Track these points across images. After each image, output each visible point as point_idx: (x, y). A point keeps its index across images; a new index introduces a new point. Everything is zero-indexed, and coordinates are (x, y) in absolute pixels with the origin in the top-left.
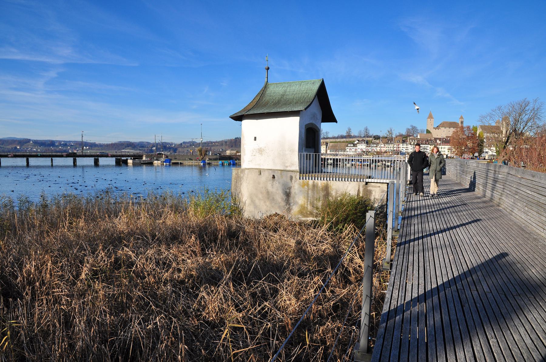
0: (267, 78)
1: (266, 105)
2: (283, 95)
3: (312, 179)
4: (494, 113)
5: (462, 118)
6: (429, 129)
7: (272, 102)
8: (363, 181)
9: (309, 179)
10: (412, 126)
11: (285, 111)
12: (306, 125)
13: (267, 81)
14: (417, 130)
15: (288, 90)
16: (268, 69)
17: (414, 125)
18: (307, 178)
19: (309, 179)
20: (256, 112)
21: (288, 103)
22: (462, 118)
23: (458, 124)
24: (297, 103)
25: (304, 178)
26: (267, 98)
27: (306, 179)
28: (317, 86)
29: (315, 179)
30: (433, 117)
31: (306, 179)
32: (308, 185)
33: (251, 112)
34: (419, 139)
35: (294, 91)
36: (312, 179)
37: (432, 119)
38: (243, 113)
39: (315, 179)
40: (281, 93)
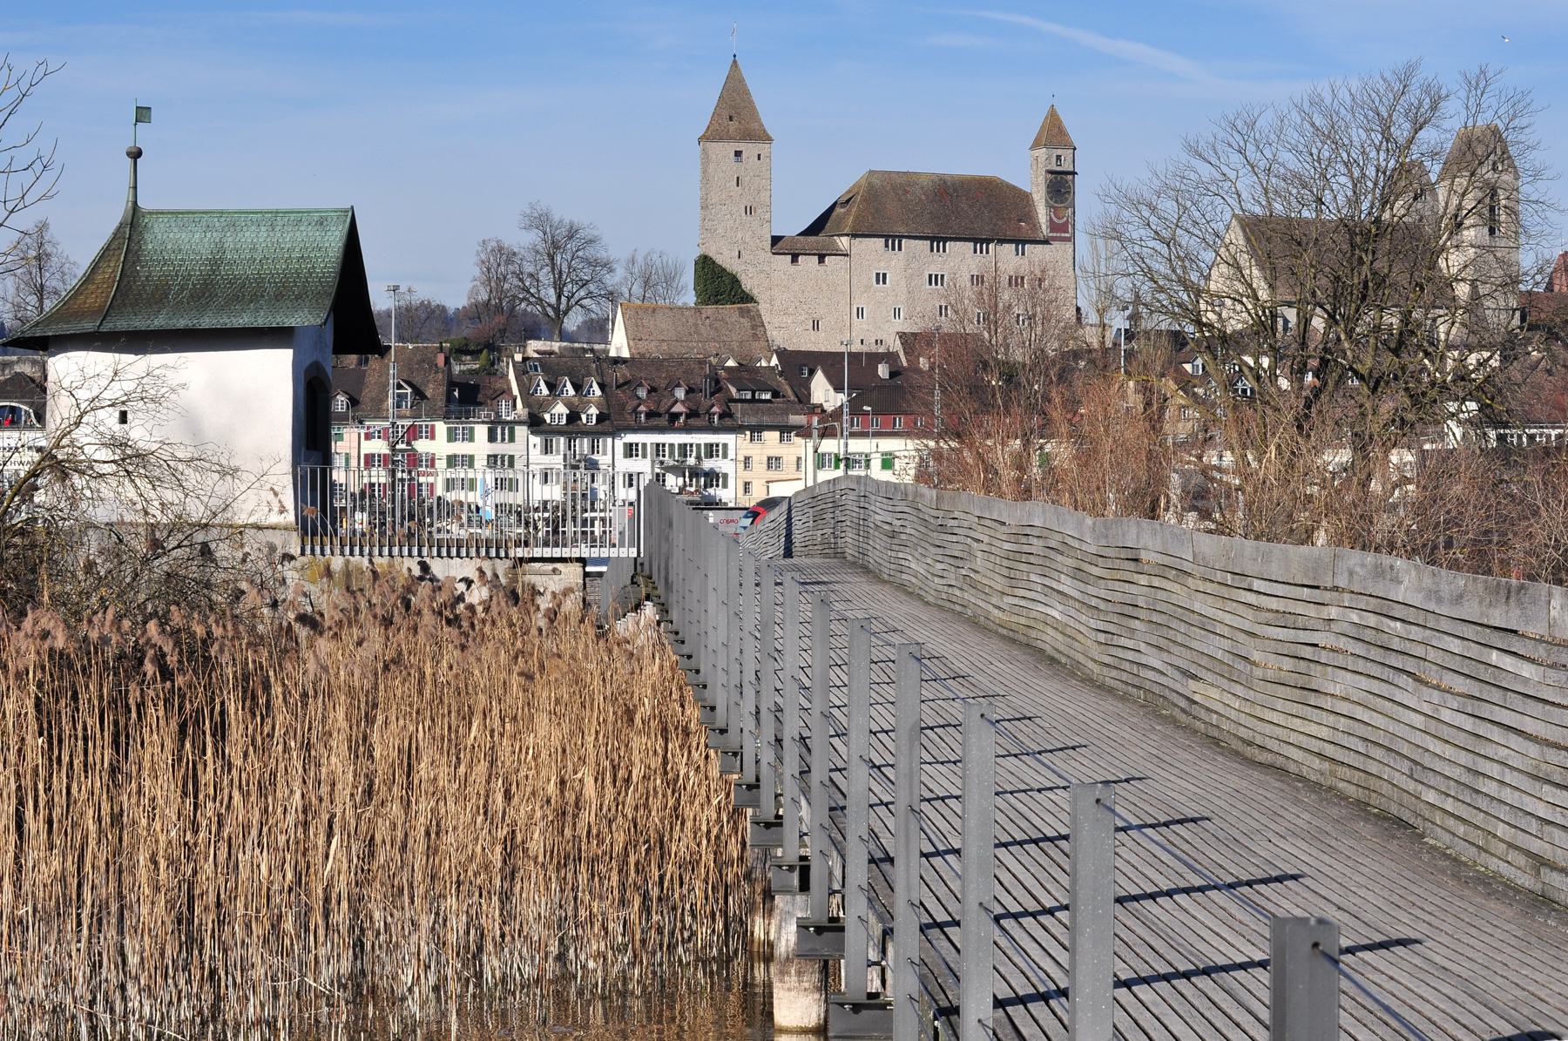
0: (135, 188)
1: (159, 297)
2: (215, 263)
3: (342, 554)
4: (1206, 171)
5: (1054, 134)
6: (726, 259)
7: (182, 289)
8: (507, 557)
9: (332, 554)
10: (540, 221)
11: (255, 325)
12: (306, 371)
13: (135, 203)
14: (594, 263)
15: (229, 243)
16: (136, 155)
17: (565, 212)
18: (328, 551)
19: (332, 554)
20: (139, 323)
21: (246, 291)
22: (1054, 134)
23: (1021, 200)
24: (279, 297)
25: (318, 549)
26: (156, 271)
27: (323, 554)
28: (337, 233)
29: (352, 554)
30: (769, 122)
31: (323, 554)
32: (328, 572)
33: (121, 324)
34: (622, 373)
35: (254, 249)
36: (342, 554)
37: (749, 149)
38: (89, 326)
39: (352, 554)
40: (206, 253)
